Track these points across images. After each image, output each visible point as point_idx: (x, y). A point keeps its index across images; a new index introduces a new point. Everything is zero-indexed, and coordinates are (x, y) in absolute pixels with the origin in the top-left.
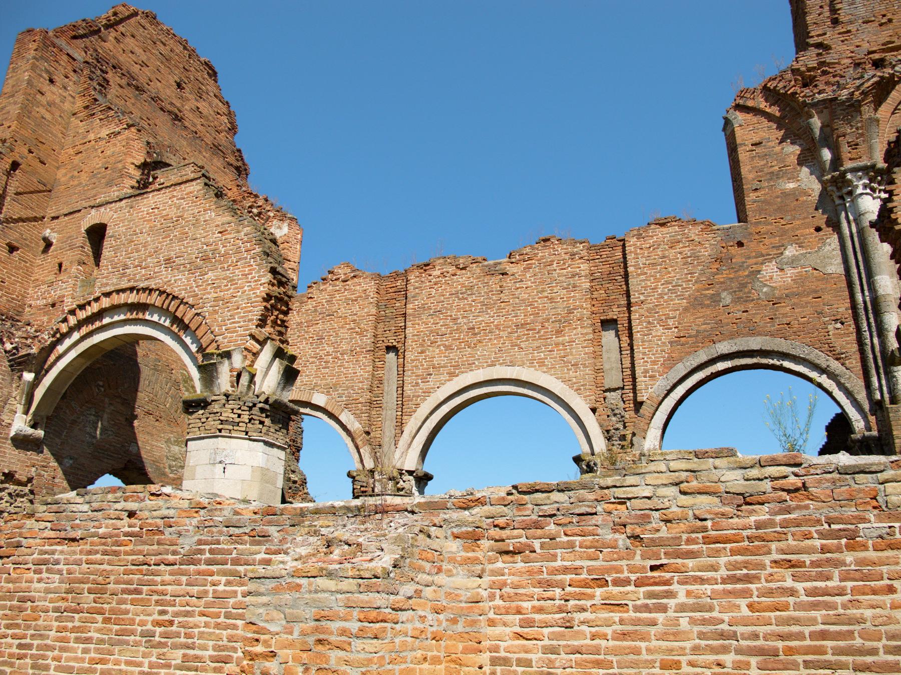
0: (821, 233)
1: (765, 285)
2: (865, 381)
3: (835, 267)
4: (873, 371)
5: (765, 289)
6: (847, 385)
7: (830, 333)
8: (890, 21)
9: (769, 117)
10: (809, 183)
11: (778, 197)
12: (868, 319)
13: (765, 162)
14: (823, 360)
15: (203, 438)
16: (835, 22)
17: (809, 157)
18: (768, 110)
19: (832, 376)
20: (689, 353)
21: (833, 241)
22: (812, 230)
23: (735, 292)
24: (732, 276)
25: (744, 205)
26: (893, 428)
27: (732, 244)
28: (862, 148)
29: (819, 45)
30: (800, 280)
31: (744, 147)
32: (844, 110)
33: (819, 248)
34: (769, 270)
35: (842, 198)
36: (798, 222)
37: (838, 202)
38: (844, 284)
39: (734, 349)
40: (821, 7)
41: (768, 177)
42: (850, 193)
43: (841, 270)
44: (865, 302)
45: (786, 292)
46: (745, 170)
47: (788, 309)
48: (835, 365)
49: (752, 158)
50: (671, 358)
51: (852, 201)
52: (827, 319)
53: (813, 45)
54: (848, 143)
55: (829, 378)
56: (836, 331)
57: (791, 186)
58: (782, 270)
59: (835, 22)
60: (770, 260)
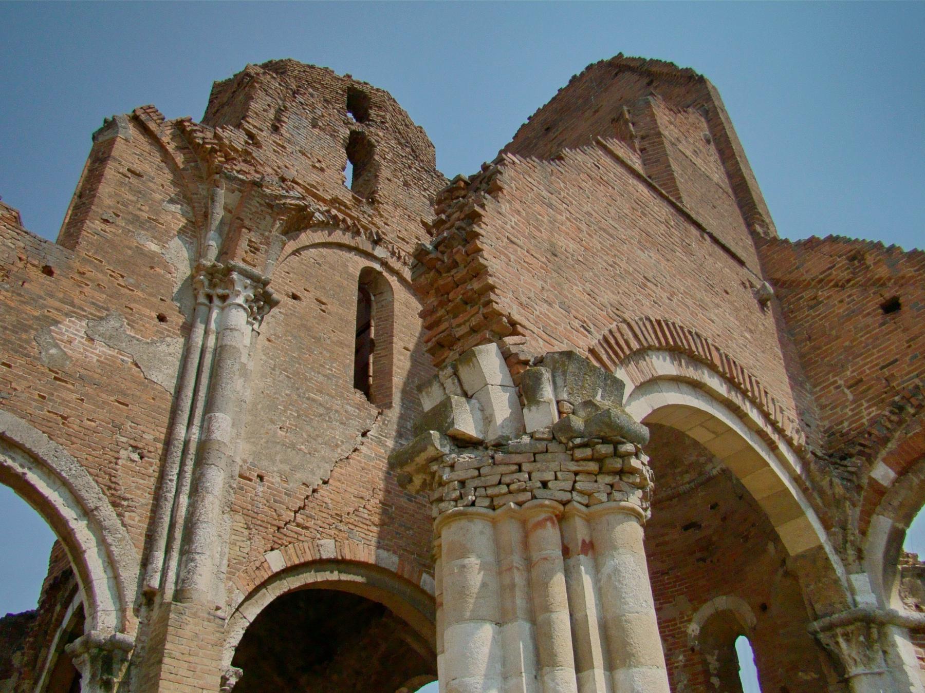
0: (163, 325)
1: (57, 346)
2: (144, 554)
3: (164, 377)
4: (162, 543)
5: (53, 351)
6: (113, 548)
7: (120, 462)
8: (322, 170)
9: (167, 157)
10: (178, 259)
11: (130, 248)
12: (183, 464)
13: (134, 199)
14: (93, 495)
16: (276, 129)
17: (195, 229)
18: (171, 148)
19: (97, 526)
22: (154, 315)
23: (6, 328)
24: (13, 305)
25: (80, 230)
26: (169, 638)
27: (36, 263)
28: (260, 256)
29: (251, 136)
31: (116, 165)
32: (260, 204)
33: (153, 342)
34: (72, 330)
35: (210, 298)
36: (140, 294)
37: (202, 299)
40: (269, 105)
41: (130, 217)
42: (224, 298)
43: (170, 385)
44: (187, 443)
45: (83, 371)
46: (105, 190)
47: (74, 396)
48: (107, 512)
49: (122, 184)
51: (223, 309)
52: (124, 440)
53: (245, 129)
54: (250, 241)
55: (89, 527)
56: (129, 464)
57: (153, 247)
58: (92, 340)
60: (81, 318)
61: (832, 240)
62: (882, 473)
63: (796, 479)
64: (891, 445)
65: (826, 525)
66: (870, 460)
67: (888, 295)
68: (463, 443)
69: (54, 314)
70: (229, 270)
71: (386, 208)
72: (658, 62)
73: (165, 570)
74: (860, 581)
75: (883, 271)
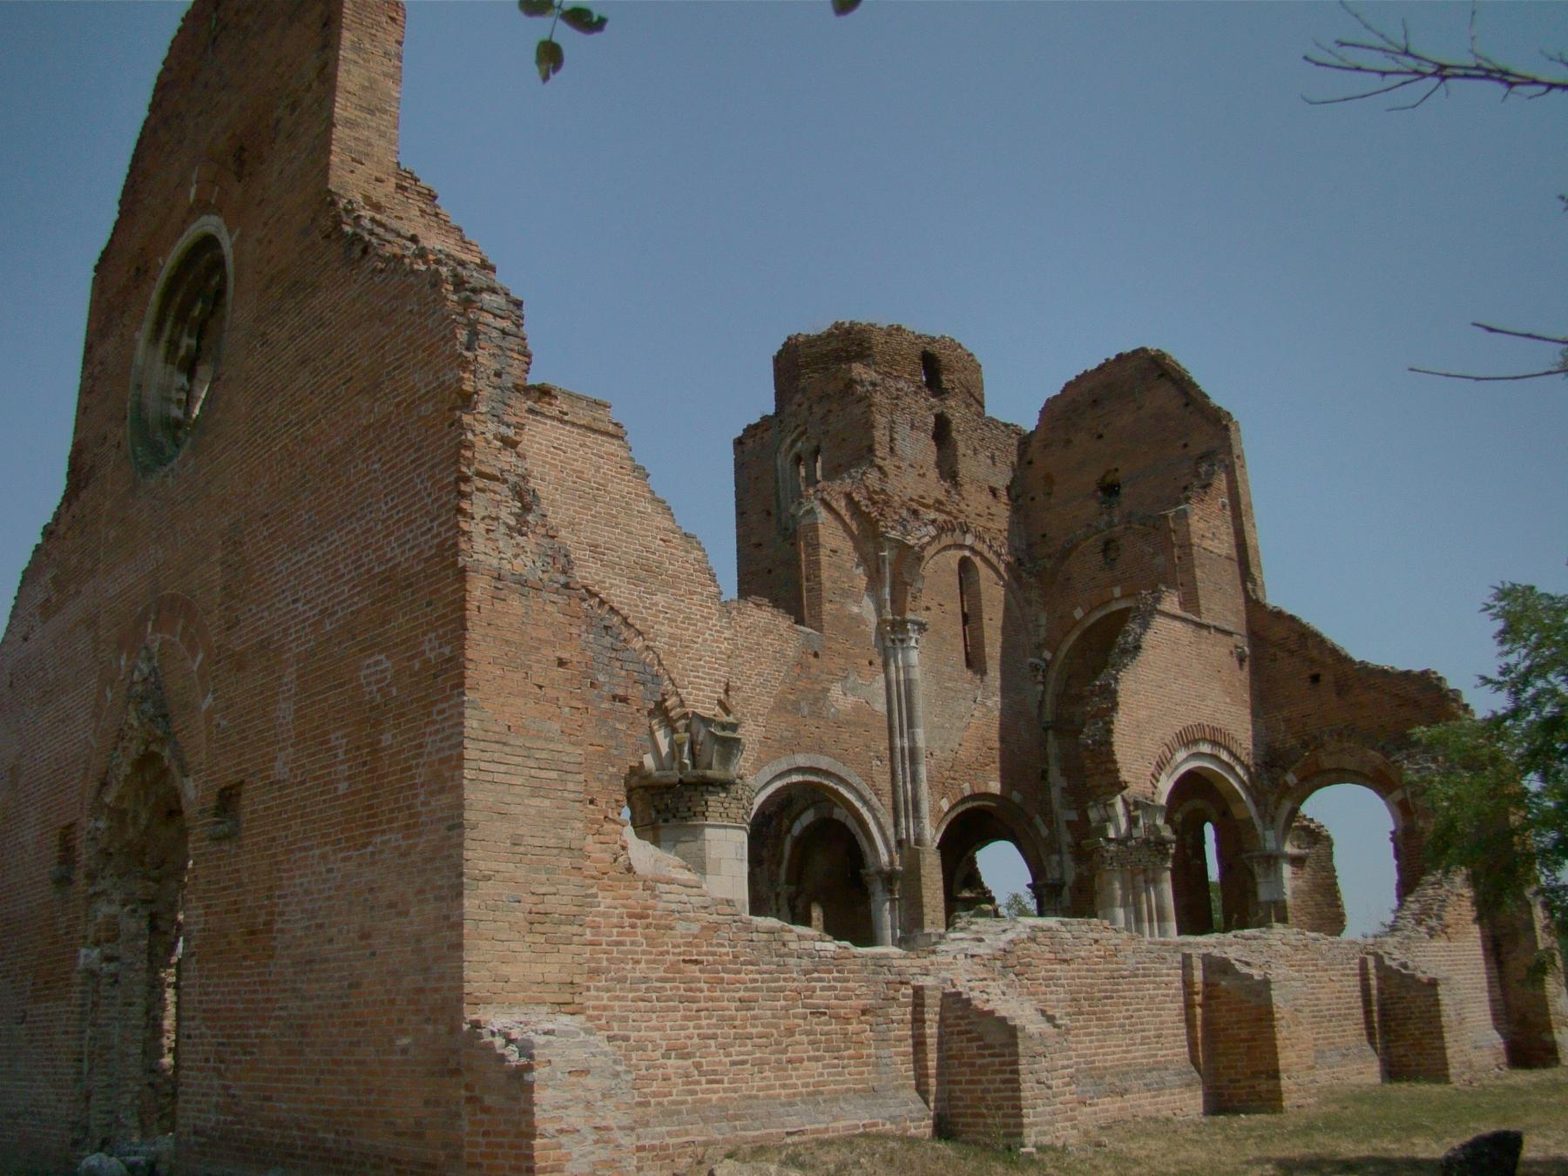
3: (880, 706)
14: (869, 794)
15: (726, 827)
16: (892, 449)
18: (847, 519)
19: (871, 809)
20: (775, 758)
21: (881, 678)
29: (880, 468)
30: (857, 709)
37: (889, 644)
38: (885, 725)
39: (808, 764)
42: (902, 641)
44: (903, 749)
48: (874, 800)
50: (758, 759)
57: (856, 610)
59: (892, 449)
61: (1292, 618)
62: (1291, 779)
63: (1242, 782)
64: (1298, 765)
65: (1257, 803)
66: (1285, 771)
67: (1316, 671)
68: (1110, 840)
69: (826, 685)
70: (904, 622)
71: (968, 488)
72: (1195, 386)
73: (908, 828)
74: (1270, 835)
75: (1315, 653)
